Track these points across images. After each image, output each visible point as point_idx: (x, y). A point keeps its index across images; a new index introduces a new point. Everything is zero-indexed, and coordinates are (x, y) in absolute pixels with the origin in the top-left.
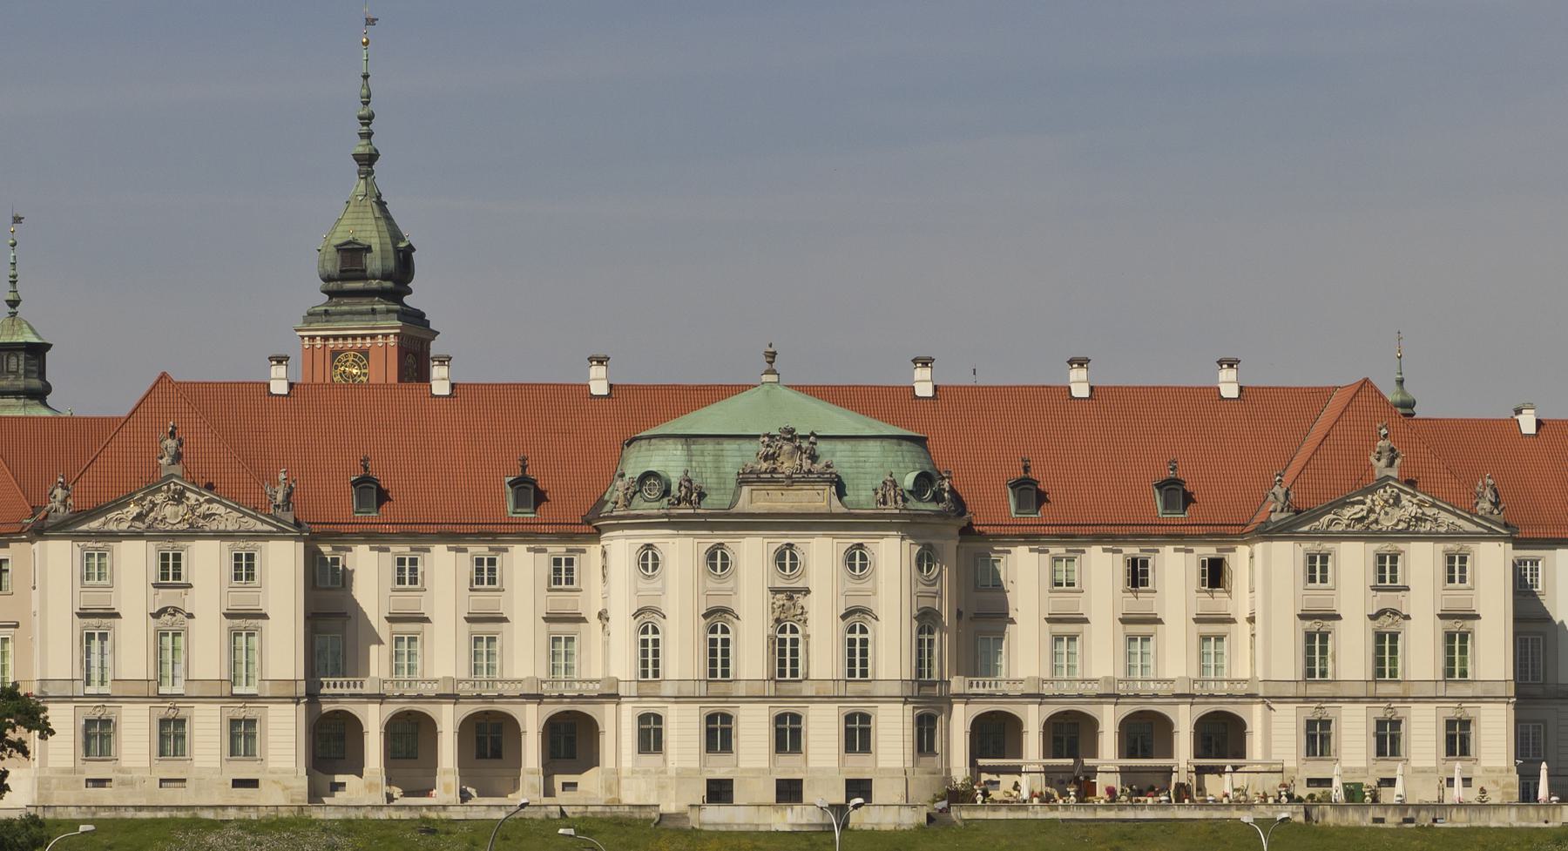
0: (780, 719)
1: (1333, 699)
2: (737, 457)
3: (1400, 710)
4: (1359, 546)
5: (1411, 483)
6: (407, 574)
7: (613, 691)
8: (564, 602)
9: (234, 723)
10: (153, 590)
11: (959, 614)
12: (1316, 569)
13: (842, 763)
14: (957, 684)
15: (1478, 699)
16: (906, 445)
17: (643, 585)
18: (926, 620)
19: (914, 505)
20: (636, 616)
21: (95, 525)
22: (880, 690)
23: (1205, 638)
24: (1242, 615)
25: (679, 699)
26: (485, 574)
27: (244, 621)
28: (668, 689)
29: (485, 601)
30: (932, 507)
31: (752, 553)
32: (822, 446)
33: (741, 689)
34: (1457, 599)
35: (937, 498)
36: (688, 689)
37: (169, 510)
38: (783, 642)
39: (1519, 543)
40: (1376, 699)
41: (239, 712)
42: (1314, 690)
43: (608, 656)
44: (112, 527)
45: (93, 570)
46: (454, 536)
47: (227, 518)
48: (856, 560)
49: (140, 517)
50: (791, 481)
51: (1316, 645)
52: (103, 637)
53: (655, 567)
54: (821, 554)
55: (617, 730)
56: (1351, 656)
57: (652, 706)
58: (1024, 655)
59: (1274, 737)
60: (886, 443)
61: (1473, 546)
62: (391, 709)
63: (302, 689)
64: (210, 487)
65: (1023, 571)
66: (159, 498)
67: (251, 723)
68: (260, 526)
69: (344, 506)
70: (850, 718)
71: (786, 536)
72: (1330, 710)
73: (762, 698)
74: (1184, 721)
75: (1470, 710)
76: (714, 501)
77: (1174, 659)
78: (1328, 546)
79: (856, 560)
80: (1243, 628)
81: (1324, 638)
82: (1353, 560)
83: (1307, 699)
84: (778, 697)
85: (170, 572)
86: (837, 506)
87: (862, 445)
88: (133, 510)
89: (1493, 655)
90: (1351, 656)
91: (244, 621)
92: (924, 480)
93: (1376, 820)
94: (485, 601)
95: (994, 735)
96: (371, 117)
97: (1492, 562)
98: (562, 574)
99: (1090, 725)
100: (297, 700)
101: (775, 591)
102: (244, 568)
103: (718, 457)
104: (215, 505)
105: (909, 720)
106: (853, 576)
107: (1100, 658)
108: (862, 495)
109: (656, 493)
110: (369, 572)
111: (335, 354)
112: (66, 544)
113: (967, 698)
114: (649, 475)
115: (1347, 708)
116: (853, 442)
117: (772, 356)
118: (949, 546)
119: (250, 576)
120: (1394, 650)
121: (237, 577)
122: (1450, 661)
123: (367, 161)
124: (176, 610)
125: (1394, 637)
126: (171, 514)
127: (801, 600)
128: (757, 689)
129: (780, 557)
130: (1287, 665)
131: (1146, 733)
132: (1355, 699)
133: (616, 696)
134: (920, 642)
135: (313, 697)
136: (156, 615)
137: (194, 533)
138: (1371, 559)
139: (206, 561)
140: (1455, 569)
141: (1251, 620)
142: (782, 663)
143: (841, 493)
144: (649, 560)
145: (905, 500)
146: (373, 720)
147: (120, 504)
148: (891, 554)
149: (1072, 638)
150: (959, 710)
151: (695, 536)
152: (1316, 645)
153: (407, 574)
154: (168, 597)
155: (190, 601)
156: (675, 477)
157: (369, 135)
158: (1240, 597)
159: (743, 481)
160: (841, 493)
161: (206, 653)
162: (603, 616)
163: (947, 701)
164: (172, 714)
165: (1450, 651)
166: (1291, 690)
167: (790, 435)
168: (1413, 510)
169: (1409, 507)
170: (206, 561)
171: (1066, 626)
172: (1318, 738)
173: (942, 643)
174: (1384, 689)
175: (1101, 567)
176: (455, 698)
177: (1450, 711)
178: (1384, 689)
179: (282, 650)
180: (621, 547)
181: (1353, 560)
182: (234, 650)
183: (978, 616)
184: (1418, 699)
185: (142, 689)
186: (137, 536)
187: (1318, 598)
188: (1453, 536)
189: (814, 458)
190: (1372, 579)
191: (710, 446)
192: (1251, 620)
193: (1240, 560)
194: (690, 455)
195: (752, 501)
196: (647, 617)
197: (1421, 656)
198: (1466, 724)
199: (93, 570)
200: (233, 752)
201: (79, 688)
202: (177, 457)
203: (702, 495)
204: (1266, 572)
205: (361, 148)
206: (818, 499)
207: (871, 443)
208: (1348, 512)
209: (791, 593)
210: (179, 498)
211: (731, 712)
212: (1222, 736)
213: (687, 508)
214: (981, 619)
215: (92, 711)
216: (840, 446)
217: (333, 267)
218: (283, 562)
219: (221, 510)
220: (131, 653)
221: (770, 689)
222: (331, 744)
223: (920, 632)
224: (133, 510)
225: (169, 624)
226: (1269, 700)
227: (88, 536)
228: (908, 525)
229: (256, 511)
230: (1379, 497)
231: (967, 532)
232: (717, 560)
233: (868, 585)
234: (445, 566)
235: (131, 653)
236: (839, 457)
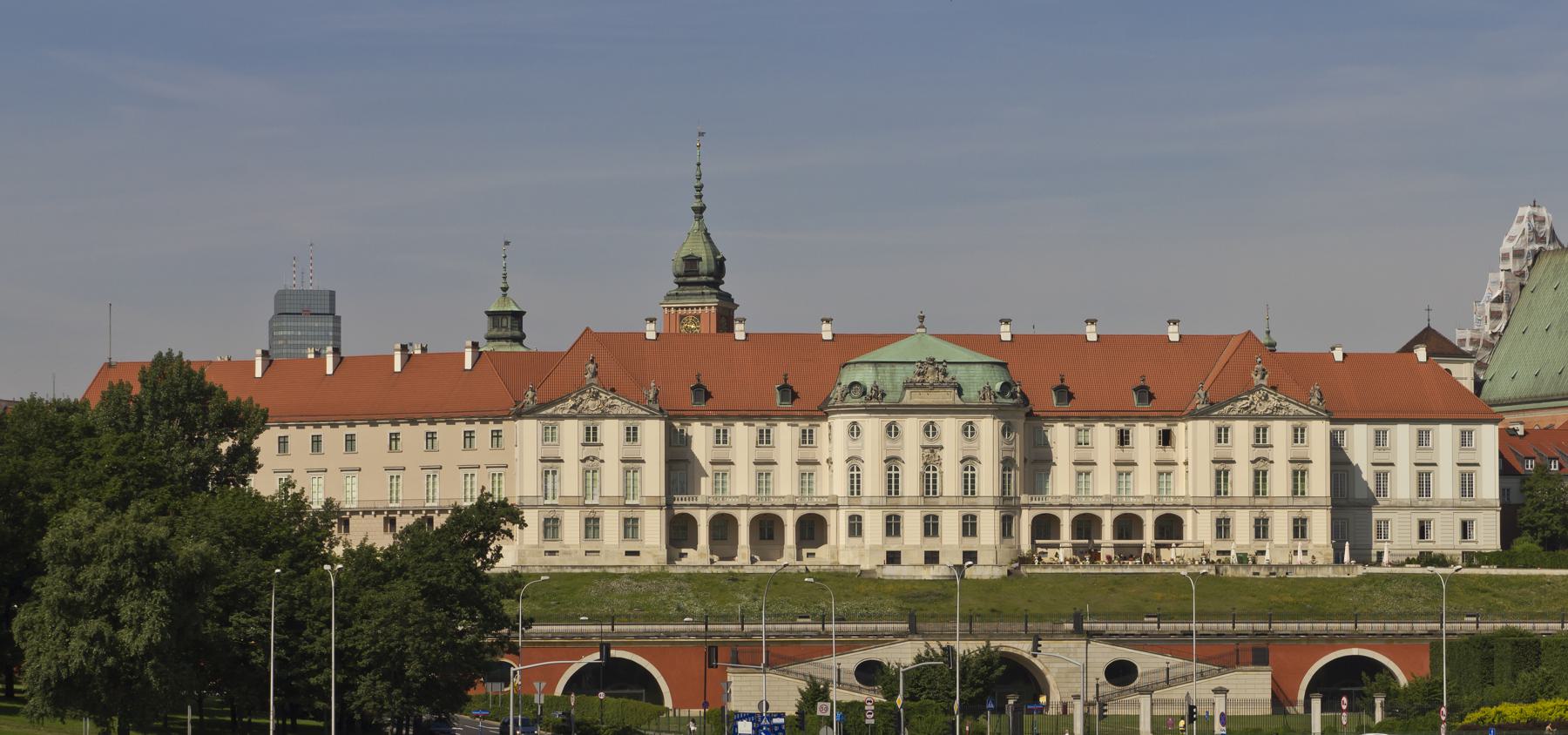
0: (927, 518)
1: (1231, 507)
2: (904, 374)
3: (1268, 513)
4: (1246, 422)
5: (1274, 388)
6: (722, 438)
8: (808, 454)
9: (626, 520)
12: (1222, 435)
13: (961, 542)
14: (1024, 499)
15: (1311, 507)
17: (851, 444)
18: (1007, 463)
19: (1001, 400)
21: (549, 411)
22: (981, 502)
23: (1161, 474)
24: (1181, 461)
25: (871, 507)
26: (764, 438)
27: (632, 464)
28: (865, 502)
29: (764, 453)
30: (1011, 401)
31: (911, 426)
32: (950, 368)
33: (905, 502)
34: (1299, 452)
35: (1013, 396)
36: (876, 501)
37: (590, 403)
39: (1333, 421)
40: (1255, 507)
41: (629, 514)
42: (1221, 502)
43: (832, 483)
45: (549, 436)
46: (747, 418)
47: (623, 408)
48: (969, 431)
49: (574, 407)
50: (933, 387)
51: (1222, 477)
52: (554, 473)
54: (950, 427)
55: (837, 523)
56: (1241, 483)
57: (857, 511)
58: (1061, 483)
59: (1198, 528)
61: (1308, 422)
62: (713, 512)
63: (663, 502)
64: (613, 390)
65: (1061, 436)
66: (585, 396)
67: (636, 520)
69: (687, 401)
70: (965, 518)
72: (1229, 513)
73: (917, 507)
74: (1149, 519)
75: (1306, 513)
76: (890, 398)
77: (1143, 485)
78: (1228, 423)
79: (969, 431)
80: (1181, 468)
81: (1226, 473)
82: (1242, 431)
83: (1217, 507)
84: (926, 506)
85: (591, 437)
86: (958, 401)
88: (571, 403)
89: (1319, 483)
90: (1241, 483)
91: (632, 464)
92: (1006, 386)
94: (764, 453)
95: (1045, 527)
97: (1319, 431)
98: (807, 438)
99: (1098, 521)
100: (661, 508)
101: (924, 448)
102: (632, 435)
103: (893, 374)
105: (998, 518)
107: (1103, 484)
108: (972, 395)
110: (700, 436)
111: (682, 317)
112: (533, 422)
113: (1029, 506)
115: (1239, 512)
117: (922, 318)
119: (635, 439)
120: (1264, 480)
122: (1296, 486)
123: (699, 211)
125: (1265, 473)
126: (591, 405)
127: (938, 453)
129: (927, 429)
130: (1206, 488)
131: (1127, 525)
132: (1243, 507)
135: (669, 506)
136: (583, 461)
137: (604, 416)
138: (1252, 430)
139: (611, 430)
140: (1298, 435)
141: (1186, 463)
143: (960, 393)
144: (854, 430)
146: (703, 518)
147: (563, 400)
148: (988, 427)
149: (1088, 473)
150: (1025, 512)
152: (1222, 477)
153: (722, 438)
154: (590, 451)
155: (602, 453)
156: (869, 385)
158: (1180, 451)
160: (960, 393)
161: (611, 482)
162: (829, 461)
163: (1019, 508)
165: (1295, 480)
166: (1208, 502)
167: (932, 362)
168: (1275, 403)
169: (1273, 401)
170: (611, 430)
171: (1084, 467)
172: (1223, 528)
173: (1016, 476)
174: (1259, 502)
175: (1103, 434)
176: (748, 506)
177: (1295, 513)
178: (1259, 502)
179: (653, 480)
180: (839, 423)
181: (1242, 431)
182: (626, 480)
183: (1035, 461)
184: (1278, 507)
187: (1223, 452)
188: (1297, 417)
189: (945, 374)
190: (1252, 441)
191: (888, 368)
192: (1186, 463)
193: (1180, 430)
195: (911, 398)
196: (853, 462)
197: (1279, 483)
198: (1304, 521)
199: (549, 436)
200: (626, 536)
201: (541, 501)
202: (595, 374)
203: (884, 395)
204: (1194, 437)
205: (696, 204)
206: (948, 397)
208: (1239, 404)
209: (933, 449)
210: (596, 396)
212: (1170, 527)
213: (875, 402)
214: (1038, 463)
215: (548, 513)
216: (960, 367)
217: (681, 269)
218: (653, 432)
219: (617, 402)
220: (570, 482)
221: (921, 501)
222: (680, 532)
224: (571, 403)
225: (591, 466)
226: (1196, 508)
227: (546, 417)
228: (997, 411)
229: (638, 403)
230: (1256, 396)
231: (1030, 415)
232: (892, 431)
233: (975, 444)
234: (742, 434)
235: (570, 482)
236: (959, 374)
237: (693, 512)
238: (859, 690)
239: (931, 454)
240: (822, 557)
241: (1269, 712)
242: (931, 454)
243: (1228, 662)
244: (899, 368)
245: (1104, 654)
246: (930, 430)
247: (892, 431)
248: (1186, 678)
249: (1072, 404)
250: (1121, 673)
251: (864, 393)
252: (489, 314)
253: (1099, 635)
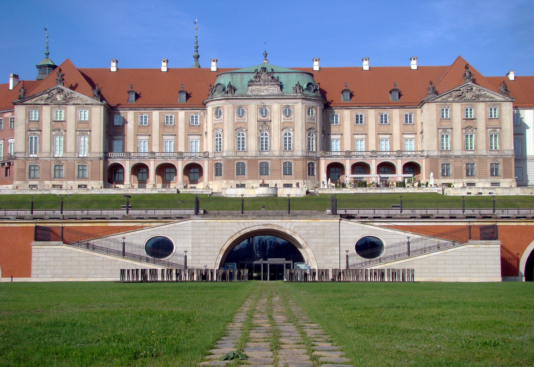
16: (304, 74)
18: (309, 130)
19: (306, 92)
30: (314, 94)
38: (262, 139)
44: (39, 102)
53: (220, 114)
60: (298, 74)
87: (290, 74)
92: (309, 84)
93: (468, 193)
95: (335, 169)
96: (198, 47)
103: (242, 79)
108: (289, 89)
109: (221, 90)
114: (219, 84)
116: (287, 74)
134: (309, 139)
135: (106, 158)
142: (262, 146)
143: (281, 87)
144: (218, 112)
145: (303, 91)
148: (299, 107)
157: (197, 51)
160: (281, 87)
175: (371, 116)
180: (210, 108)
191: (239, 76)
194: (232, 78)
204: (427, 115)
206: (275, 90)
207: (293, 75)
209: (264, 122)
210: (60, 91)
218: (97, 115)
222: (113, 174)
232: (241, 112)
236: (283, 78)
238: (147, 260)
239: (264, 124)
240: (200, 188)
241: (499, 279)
242: (264, 124)
243: (459, 237)
244: (246, 76)
245: (355, 231)
246: (263, 111)
247: (241, 112)
248: (424, 251)
249: (354, 99)
250: (369, 248)
251: (224, 90)
252: (39, 67)
253: (350, 217)
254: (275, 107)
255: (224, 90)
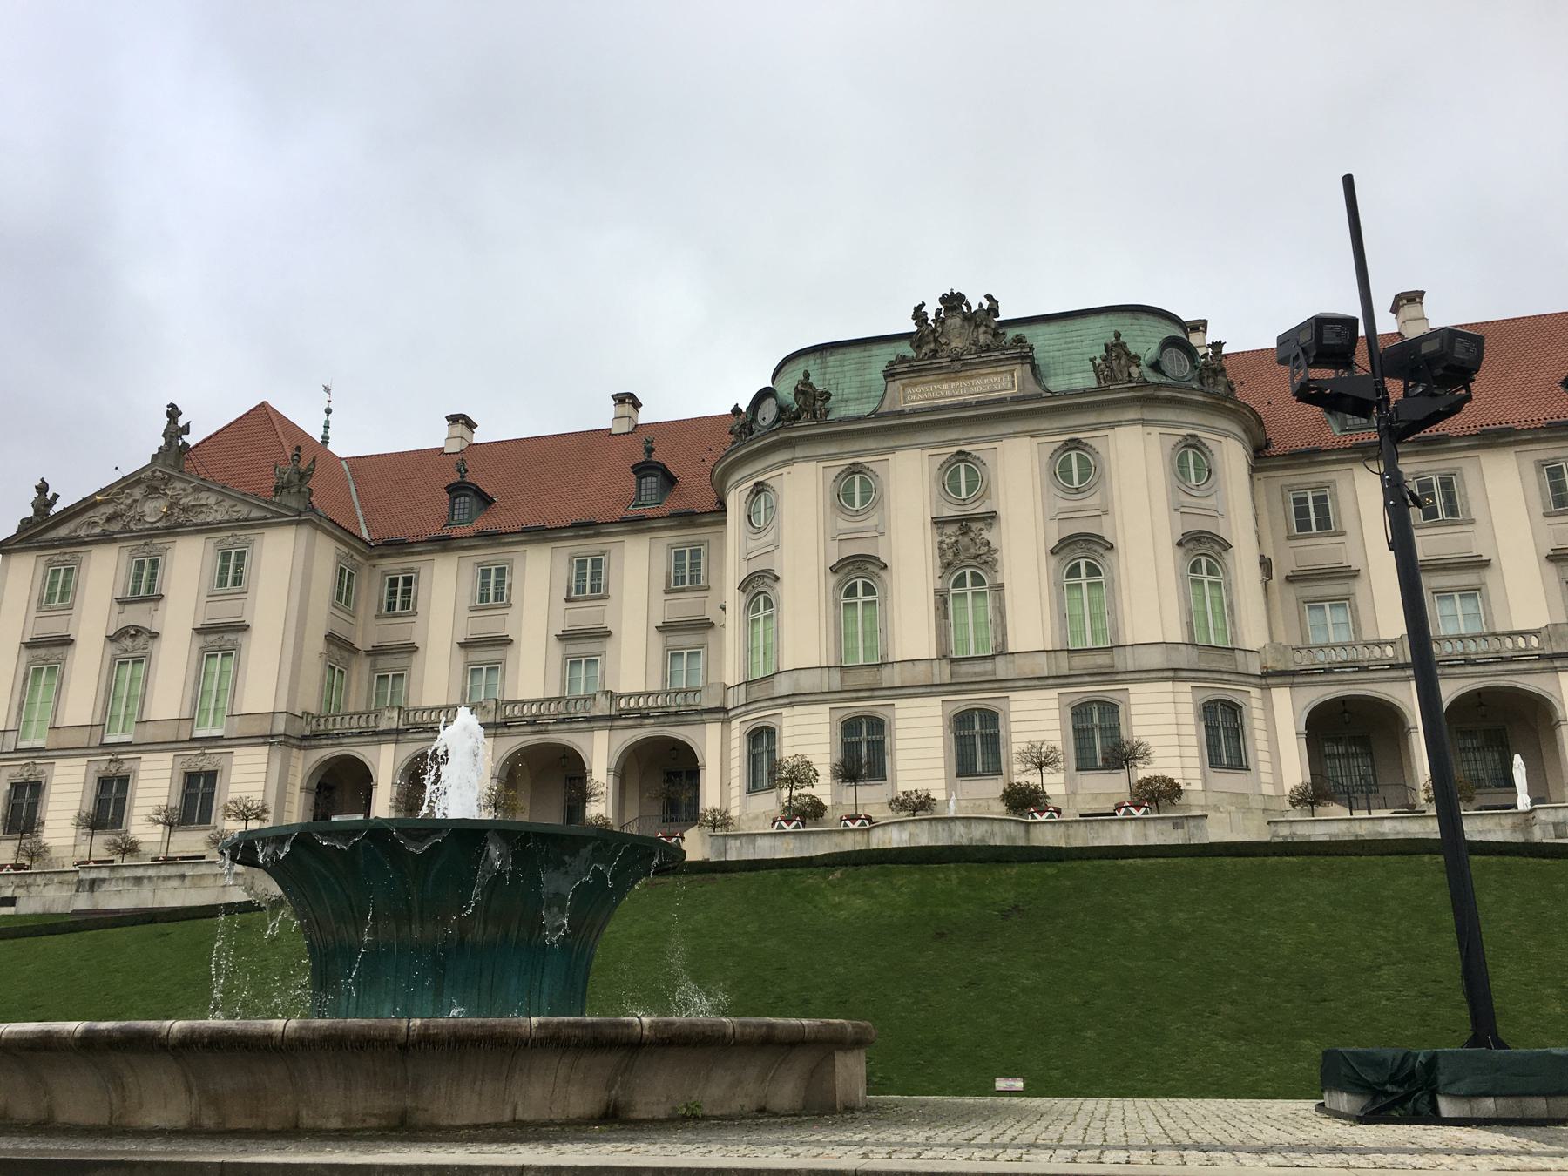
7: (717, 704)
10: (117, 608)
11: (1265, 564)
20: (743, 587)
21: (63, 531)
28: (783, 686)
29: (585, 615)
31: (910, 480)
32: (1011, 333)
36: (808, 683)
50: (958, 365)
57: (761, 716)
68: (255, 513)
71: (956, 442)
100: (267, 739)
101: (939, 522)
104: (204, 495)
106: (1066, 490)
118: (1232, 456)
121: (222, 582)
124: (139, 631)
126: (153, 510)
128: (920, 674)
133: (724, 710)
151: (818, 458)
154: (136, 615)
159: (889, 375)
164: (113, 768)
180: (736, 502)
185: (81, 739)
186: (106, 539)
209: (964, 524)
211: (882, 713)
216: (1041, 329)
221: (943, 673)
223: (1195, 568)
227: (52, 545)
237: (364, 753)
246: (961, 473)
254: (1017, 469)
255: (782, 409)
